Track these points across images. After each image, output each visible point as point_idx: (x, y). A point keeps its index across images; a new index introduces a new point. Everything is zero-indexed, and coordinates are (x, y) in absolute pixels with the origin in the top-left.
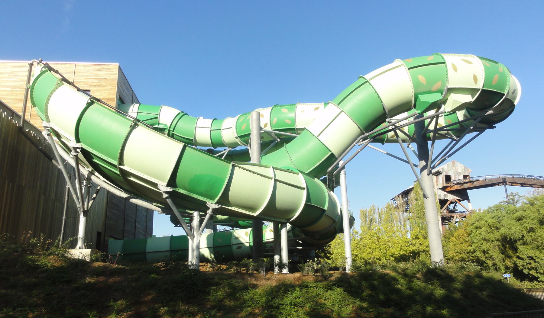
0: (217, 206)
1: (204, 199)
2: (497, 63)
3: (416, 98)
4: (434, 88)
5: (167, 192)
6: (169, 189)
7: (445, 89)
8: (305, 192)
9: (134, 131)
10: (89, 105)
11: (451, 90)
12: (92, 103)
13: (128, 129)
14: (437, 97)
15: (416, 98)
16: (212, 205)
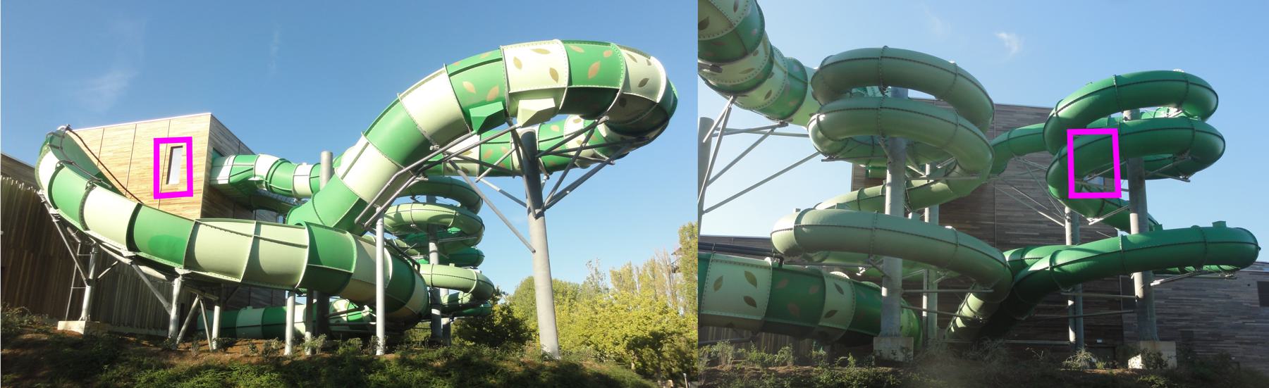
0: (187, 272)
1: (172, 264)
2: (608, 44)
3: (466, 113)
4: (489, 97)
5: (130, 257)
6: (131, 254)
7: (506, 96)
8: (306, 252)
9: (92, 193)
10: (58, 169)
11: (515, 96)
12: (62, 167)
13: (84, 191)
14: (498, 107)
15: (466, 113)
16: (181, 270)
